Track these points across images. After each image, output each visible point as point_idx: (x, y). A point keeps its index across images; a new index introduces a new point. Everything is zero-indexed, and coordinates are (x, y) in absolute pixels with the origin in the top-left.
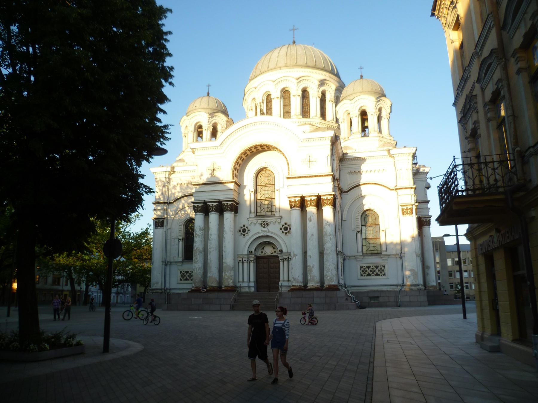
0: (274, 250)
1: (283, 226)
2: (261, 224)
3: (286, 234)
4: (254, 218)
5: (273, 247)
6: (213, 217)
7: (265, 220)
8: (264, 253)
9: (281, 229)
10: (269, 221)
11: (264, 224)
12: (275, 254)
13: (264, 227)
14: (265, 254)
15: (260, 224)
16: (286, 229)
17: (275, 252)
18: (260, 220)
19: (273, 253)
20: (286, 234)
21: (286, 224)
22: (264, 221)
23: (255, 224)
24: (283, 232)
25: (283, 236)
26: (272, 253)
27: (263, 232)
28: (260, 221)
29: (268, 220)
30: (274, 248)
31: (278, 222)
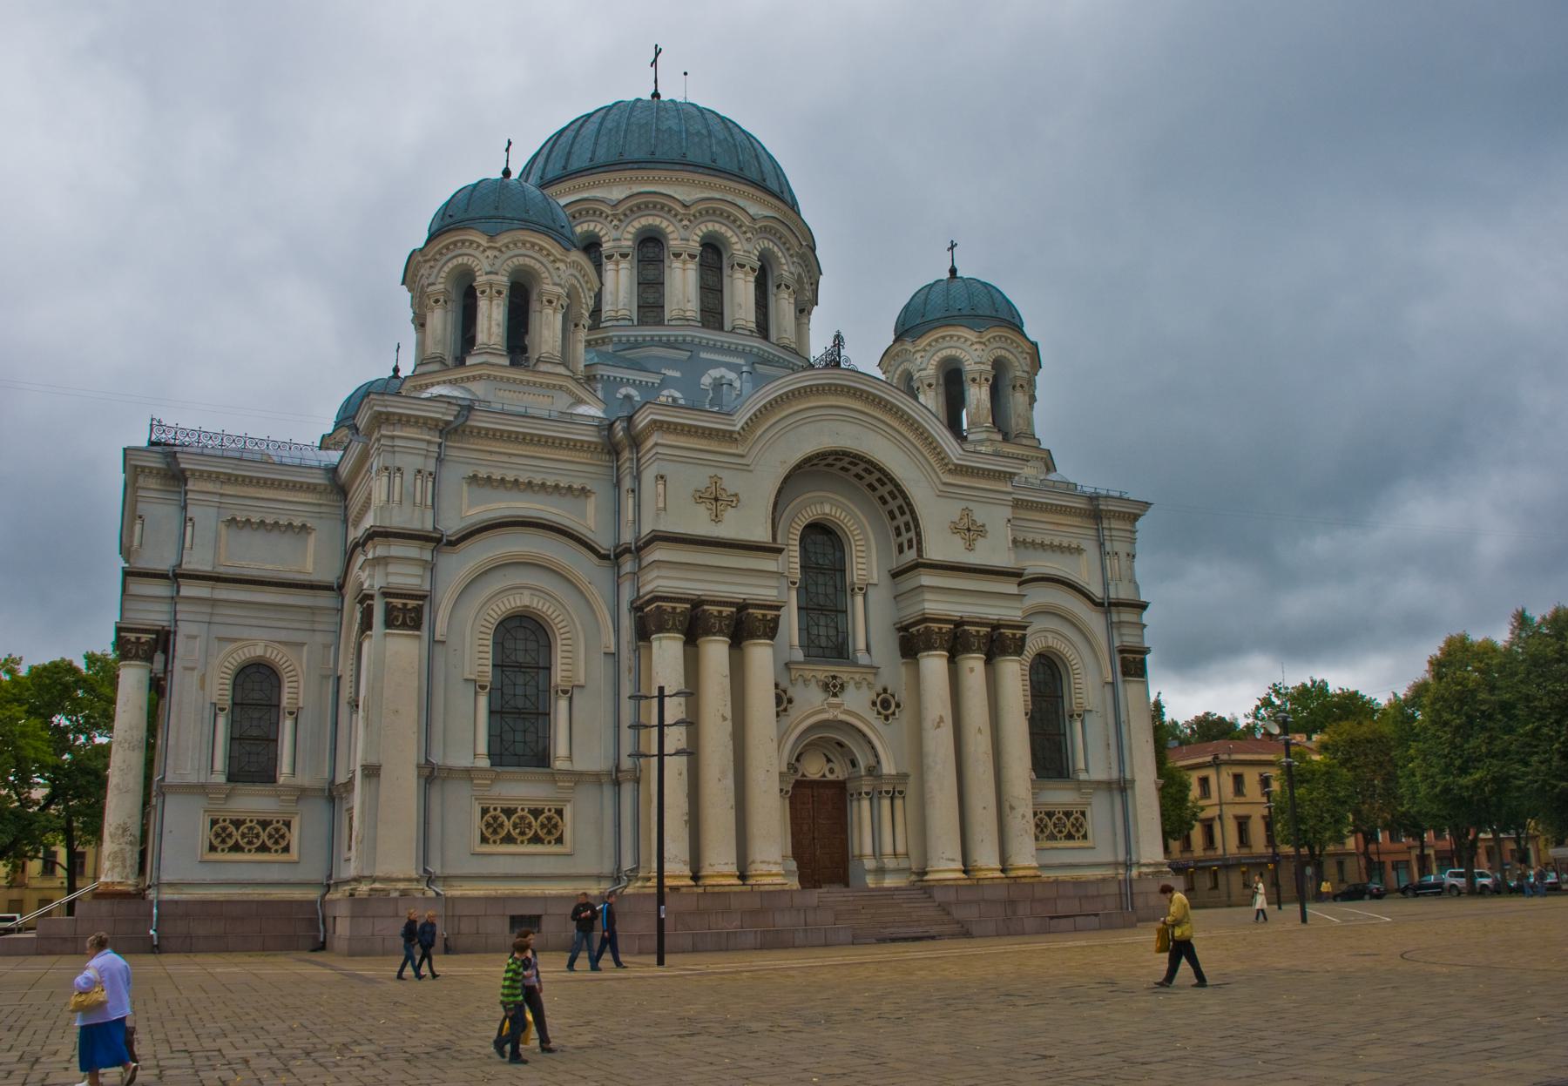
0: (831, 765)
1: (878, 695)
2: (826, 687)
3: (887, 718)
4: (805, 663)
5: (826, 756)
6: (716, 651)
7: (836, 674)
8: (800, 774)
9: (874, 704)
10: (845, 677)
11: (835, 686)
12: (830, 777)
13: (835, 695)
14: (803, 775)
15: (821, 684)
16: (885, 704)
17: (832, 771)
18: (823, 671)
19: (827, 774)
20: (887, 718)
21: (885, 691)
22: (834, 677)
23: (806, 682)
24: (879, 713)
25: (878, 723)
26: (824, 776)
27: (831, 710)
28: (821, 676)
29: (843, 672)
30: (829, 760)
31: (869, 683)
